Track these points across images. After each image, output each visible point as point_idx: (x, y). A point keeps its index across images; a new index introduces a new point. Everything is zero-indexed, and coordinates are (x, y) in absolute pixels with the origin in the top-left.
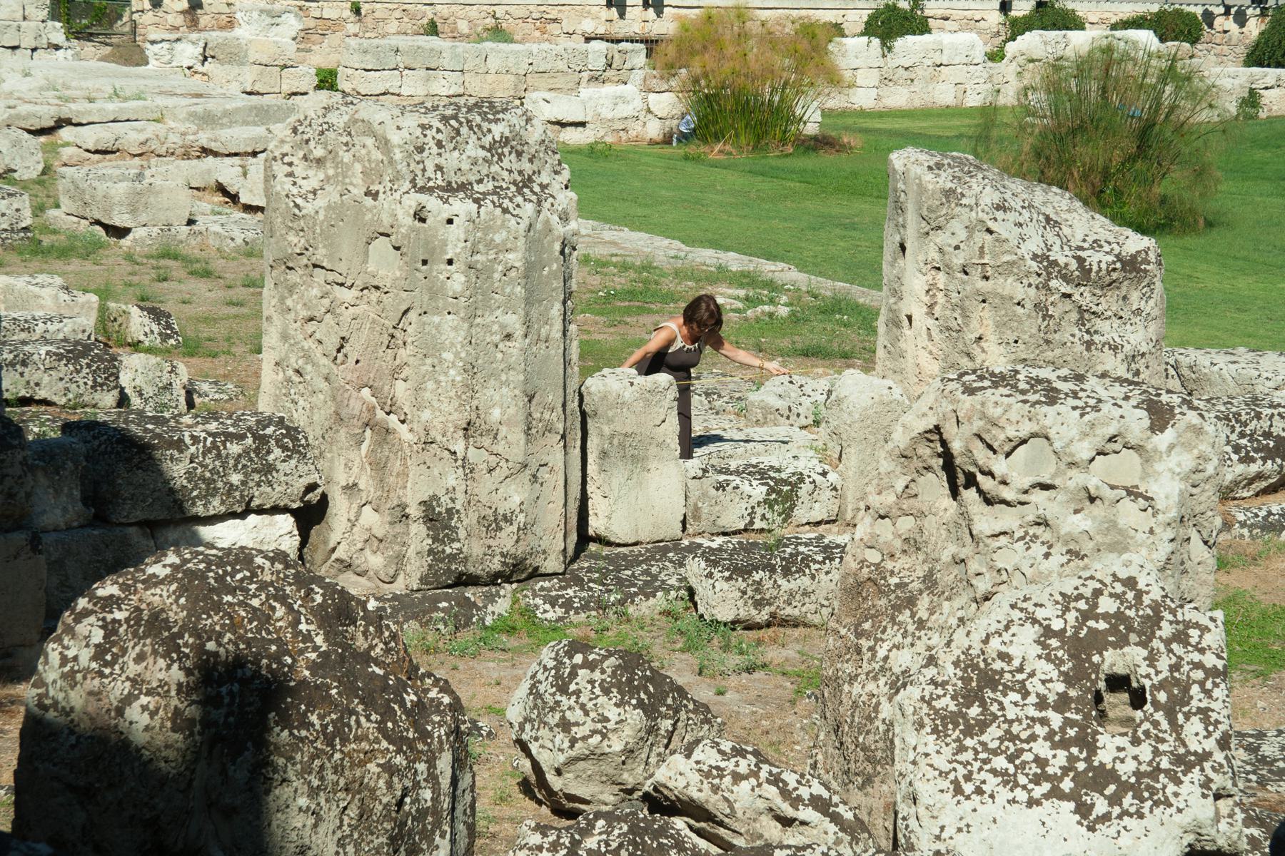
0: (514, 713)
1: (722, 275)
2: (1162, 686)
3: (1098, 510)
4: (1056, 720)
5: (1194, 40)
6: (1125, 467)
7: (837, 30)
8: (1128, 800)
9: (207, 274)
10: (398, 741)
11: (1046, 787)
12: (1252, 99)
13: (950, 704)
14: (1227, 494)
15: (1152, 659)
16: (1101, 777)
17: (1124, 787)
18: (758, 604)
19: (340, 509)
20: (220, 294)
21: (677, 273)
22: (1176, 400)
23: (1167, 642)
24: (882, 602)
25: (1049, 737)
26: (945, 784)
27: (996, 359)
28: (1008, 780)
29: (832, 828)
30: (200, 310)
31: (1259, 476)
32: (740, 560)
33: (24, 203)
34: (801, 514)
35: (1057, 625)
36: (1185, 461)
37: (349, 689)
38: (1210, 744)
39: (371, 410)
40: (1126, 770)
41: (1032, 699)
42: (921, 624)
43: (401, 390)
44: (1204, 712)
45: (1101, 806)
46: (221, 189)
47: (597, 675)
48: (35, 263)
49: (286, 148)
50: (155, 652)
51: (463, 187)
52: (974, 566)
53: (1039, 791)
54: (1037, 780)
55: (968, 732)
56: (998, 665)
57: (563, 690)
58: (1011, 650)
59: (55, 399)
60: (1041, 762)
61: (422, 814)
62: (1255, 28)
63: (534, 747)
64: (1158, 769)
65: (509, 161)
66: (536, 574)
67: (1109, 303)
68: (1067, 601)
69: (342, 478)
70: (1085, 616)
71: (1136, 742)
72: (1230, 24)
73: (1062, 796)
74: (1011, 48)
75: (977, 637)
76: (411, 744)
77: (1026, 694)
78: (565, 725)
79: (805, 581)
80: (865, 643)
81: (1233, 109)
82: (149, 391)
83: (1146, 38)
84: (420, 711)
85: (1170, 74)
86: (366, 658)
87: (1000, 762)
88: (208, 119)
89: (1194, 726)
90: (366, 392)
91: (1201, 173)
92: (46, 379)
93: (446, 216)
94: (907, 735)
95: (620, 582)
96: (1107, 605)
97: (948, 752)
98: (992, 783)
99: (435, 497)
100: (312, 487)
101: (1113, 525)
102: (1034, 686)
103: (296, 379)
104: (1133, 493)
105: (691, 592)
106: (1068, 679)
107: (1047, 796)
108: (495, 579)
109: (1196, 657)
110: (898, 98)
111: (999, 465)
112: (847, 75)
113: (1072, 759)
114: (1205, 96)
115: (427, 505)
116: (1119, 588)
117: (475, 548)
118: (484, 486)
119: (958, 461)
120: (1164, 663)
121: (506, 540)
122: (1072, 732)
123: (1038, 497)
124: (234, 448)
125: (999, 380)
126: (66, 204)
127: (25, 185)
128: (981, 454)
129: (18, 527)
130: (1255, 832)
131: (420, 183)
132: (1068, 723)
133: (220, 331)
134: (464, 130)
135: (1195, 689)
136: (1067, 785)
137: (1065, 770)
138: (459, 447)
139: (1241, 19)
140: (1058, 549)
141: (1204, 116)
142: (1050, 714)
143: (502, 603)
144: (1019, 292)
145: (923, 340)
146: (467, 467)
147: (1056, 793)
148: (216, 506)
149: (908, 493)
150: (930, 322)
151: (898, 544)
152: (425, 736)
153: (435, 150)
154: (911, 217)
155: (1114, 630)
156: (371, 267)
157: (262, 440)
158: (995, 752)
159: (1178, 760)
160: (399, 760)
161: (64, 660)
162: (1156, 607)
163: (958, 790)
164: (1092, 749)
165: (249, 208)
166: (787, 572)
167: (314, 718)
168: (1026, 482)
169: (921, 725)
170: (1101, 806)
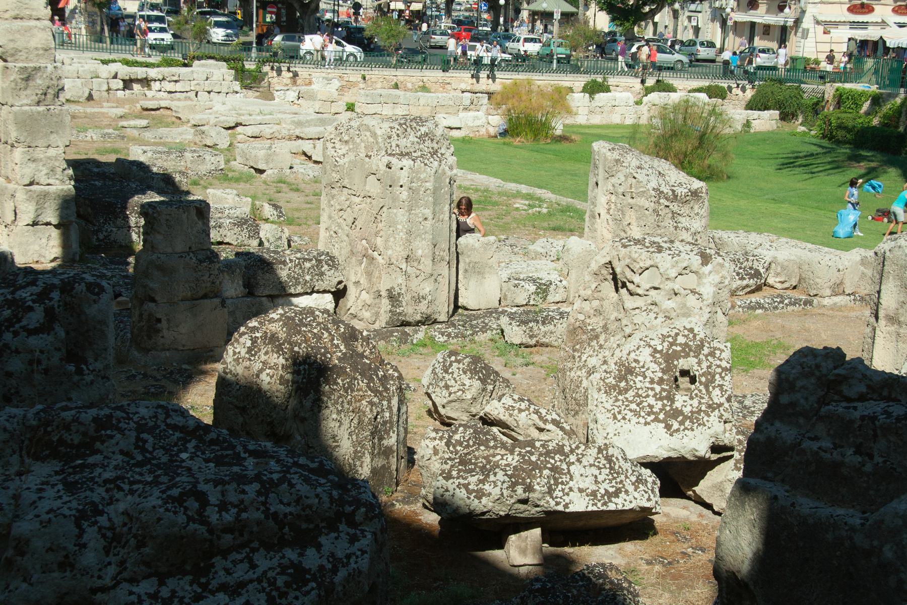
0: (425, 381)
1: (518, 195)
2: (703, 375)
3: (678, 298)
4: (658, 388)
5: (724, 98)
6: (690, 281)
7: (571, 90)
9: (297, 190)
10: (375, 392)
11: (653, 417)
12: (748, 124)
13: (611, 381)
14: (733, 293)
15: (699, 363)
16: (676, 413)
17: (686, 418)
18: (531, 337)
19: (352, 292)
20: (303, 199)
21: (499, 193)
22: (713, 252)
23: (706, 356)
24: (585, 337)
25: (655, 395)
26: (610, 415)
27: (636, 233)
28: (637, 414)
29: (561, 433)
30: (295, 205)
31: (747, 286)
32: (524, 318)
33: (221, 158)
34: (550, 298)
35: (659, 348)
36: (716, 278)
37: (355, 369)
38: (723, 400)
39: (366, 249)
40: (687, 410)
41: (648, 379)
42: (601, 347)
43: (379, 241)
44: (721, 386)
45: (676, 425)
46: (305, 154)
47: (461, 366)
48: (226, 184)
49: (332, 136)
50: (273, 351)
51: (407, 154)
52: (624, 322)
53: (649, 419)
54: (649, 414)
55: (620, 393)
56: (634, 365)
57: (446, 371)
58: (639, 358)
59: (232, 242)
61: (385, 423)
62: (749, 93)
63: (433, 396)
64: (700, 410)
65: (428, 143)
66: (435, 322)
67: (685, 210)
68: (664, 338)
69: (353, 279)
70: (672, 344)
71: (691, 398)
72: (739, 92)
73: (659, 421)
74: (645, 99)
75: (625, 352)
76: (381, 393)
77: (645, 377)
78: (447, 387)
79: (552, 327)
80: (577, 354)
81: (739, 128)
82: (272, 240)
83: (703, 96)
84: (385, 379)
85: (713, 112)
86: (362, 356)
87: (633, 406)
88: (299, 124)
89: (717, 392)
90: (364, 242)
91: (725, 155)
92: (229, 234)
93: (400, 166)
94: (594, 394)
95: (472, 326)
96: (681, 340)
97: (611, 401)
98: (630, 415)
99: (393, 288)
100: (340, 282)
101: (684, 305)
102: (649, 374)
103: (334, 235)
104: (693, 292)
105: (502, 331)
106: (664, 371)
107: (653, 421)
108: (418, 323)
109: (718, 362)
110: (596, 120)
111: (636, 279)
112: (574, 109)
113: (664, 405)
114: (727, 122)
115: (389, 291)
116: (686, 332)
117: (409, 310)
118: (413, 284)
119: (619, 277)
120: (705, 365)
121: (423, 307)
122: (664, 394)
123: (653, 293)
124: (308, 265)
125: (637, 242)
126: (238, 158)
127: (222, 151)
128: (629, 274)
129: (216, 296)
130: (741, 437)
131: (389, 152)
132: (663, 390)
133: (303, 214)
134: (409, 129)
135: (717, 376)
136: (661, 416)
137: (661, 410)
138: (404, 266)
139: (744, 90)
140: (661, 315)
141: (727, 131)
142: (655, 386)
143: (421, 334)
144: (647, 204)
146: (407, 276)
147: (656, 420)
148: (299, 289)
149: (597, 290)
150: (608, 217)
151: (592, 312)
152: (387, 390)
153: (396, 138)
154: (601, 171)
155: (683, 350)
156: (367, 188)
158: (631, 402)
159: (709, 406)
160: (376, 400)
161: (235, 353)
162: (702, 341)
163: (615, 418)
164: (673, 401)
165: (316, 162)
166: (544, 323)
167: (339, 381)
168: (648, 286)
169: (600, 390)
170: (676, 425)
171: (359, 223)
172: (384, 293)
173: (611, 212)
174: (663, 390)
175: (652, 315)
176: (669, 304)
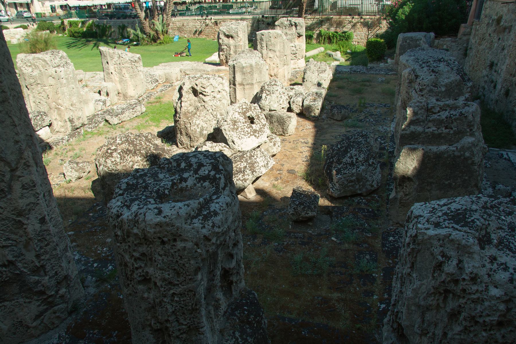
4: (246, 125)
8: (260, 133)
13: (232, 127)
15: (253, 113)
16: (255, 131)
17: (259, 131)
18: (120, 120)
19: (55, 124)
26: (237, 138)
35: (240, 111)
39: (56, 106)
40: (258, 129)
41: (242, 123)
42: (199, 116)
43: (60, 101)
45: (257, 135)
50: (133, 156)
52: (206, 106)
54: (248, 134)
55: (236, 130)
56: (235, 119)
58: (236, 117)
60: (247, 131)
68: (239, 107)
70: (242, 109)
73: (252, 135)
75: (231, 116)
87: (242, 133)
90: (54, 103)
96: (244, 107)
97: (235, 133)
98: (243, 136)
99: (70, 117)
100: (50, 121)
102: (241, 121)
103: (39, 104)
109: (258, 111)
113: (251, 130)
120: (255, 113)
124: (38, 118)
135: (260, 115)
136: (252, 133)
137: (251, 131)
138: (71, 108)
142: (245, 124)
145: (115, 75)
147: (251, 135)
148: (39, 128)
150: (116, 73)
151: (188, 105)
155: (246, 110)
157: (41, 115)
159: (263, 126)
161: (112, 162)
163: (239, 139)
169: (230, 131)
171: (50, 96)
172: (67, 120)
173: (116, 71)
174: (248, 125)
175: (215, 101)
176: (218, 96)
